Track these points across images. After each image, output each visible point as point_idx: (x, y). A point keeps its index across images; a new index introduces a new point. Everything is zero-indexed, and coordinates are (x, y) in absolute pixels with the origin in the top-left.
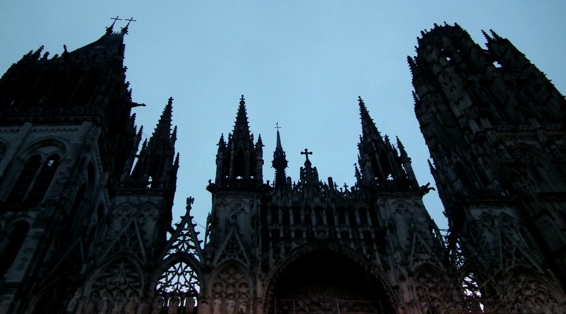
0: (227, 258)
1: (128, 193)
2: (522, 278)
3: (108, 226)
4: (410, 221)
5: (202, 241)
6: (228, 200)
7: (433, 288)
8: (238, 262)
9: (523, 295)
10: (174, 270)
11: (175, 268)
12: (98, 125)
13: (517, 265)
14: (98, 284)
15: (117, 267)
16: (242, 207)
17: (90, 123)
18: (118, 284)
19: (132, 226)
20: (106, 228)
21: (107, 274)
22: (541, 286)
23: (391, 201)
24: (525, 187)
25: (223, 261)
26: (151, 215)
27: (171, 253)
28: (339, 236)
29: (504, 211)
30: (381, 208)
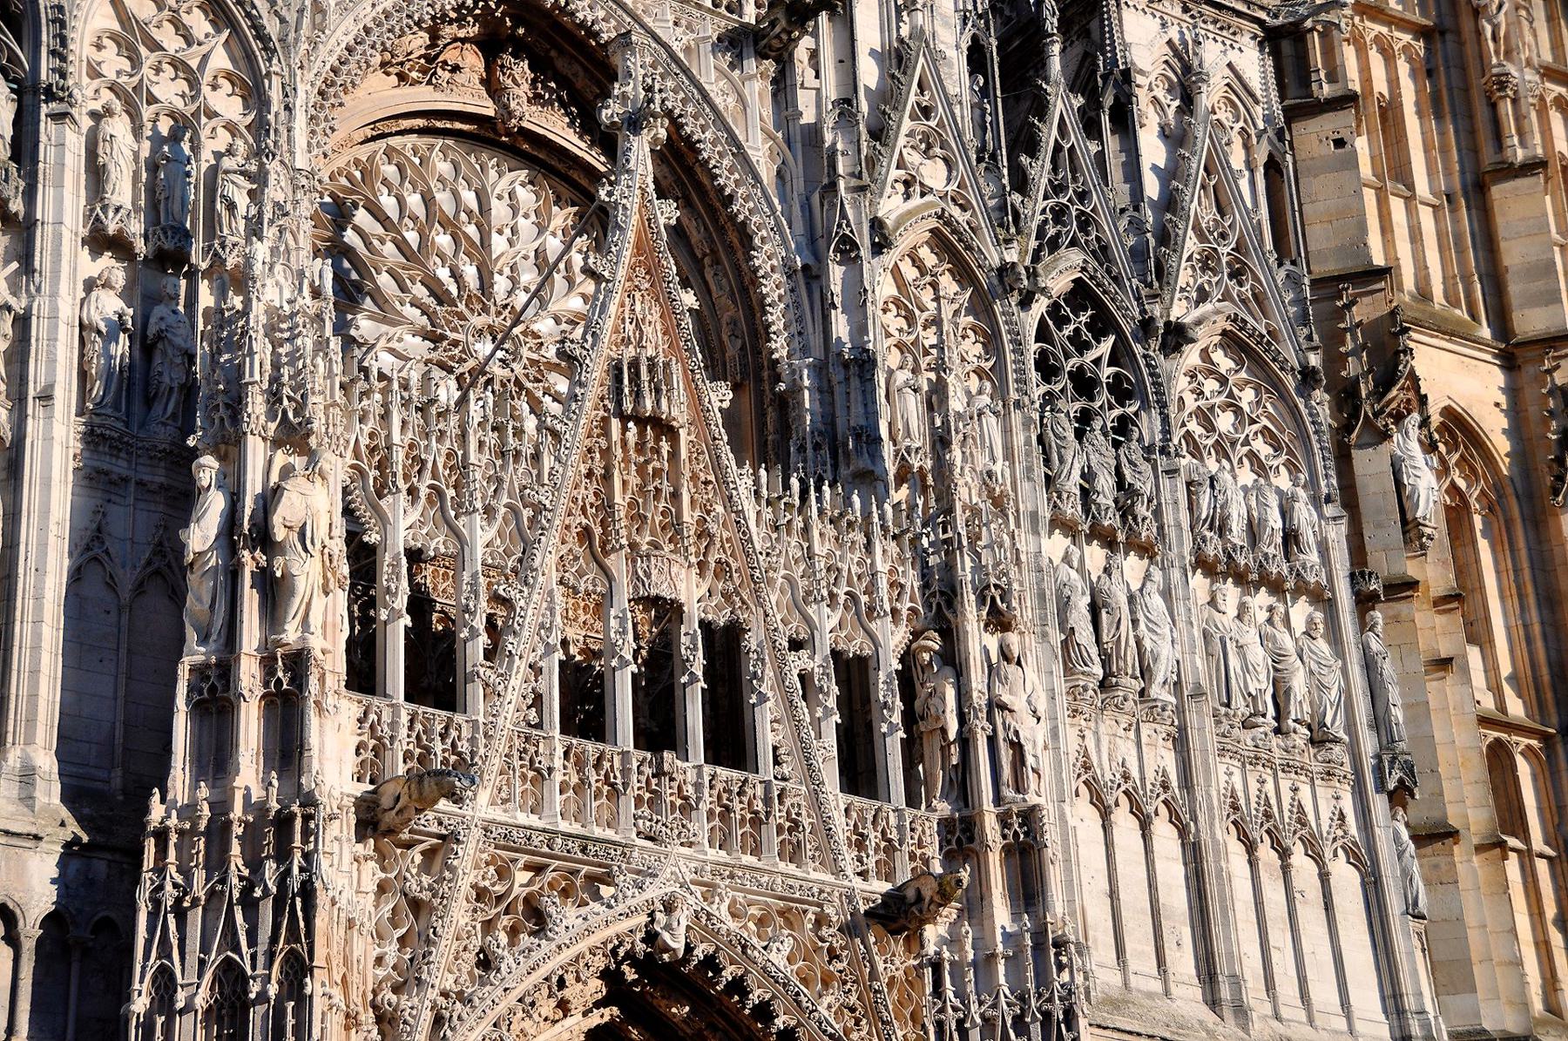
2: (1224, 362)
9: (1210, 427)
29: (1233, 56)
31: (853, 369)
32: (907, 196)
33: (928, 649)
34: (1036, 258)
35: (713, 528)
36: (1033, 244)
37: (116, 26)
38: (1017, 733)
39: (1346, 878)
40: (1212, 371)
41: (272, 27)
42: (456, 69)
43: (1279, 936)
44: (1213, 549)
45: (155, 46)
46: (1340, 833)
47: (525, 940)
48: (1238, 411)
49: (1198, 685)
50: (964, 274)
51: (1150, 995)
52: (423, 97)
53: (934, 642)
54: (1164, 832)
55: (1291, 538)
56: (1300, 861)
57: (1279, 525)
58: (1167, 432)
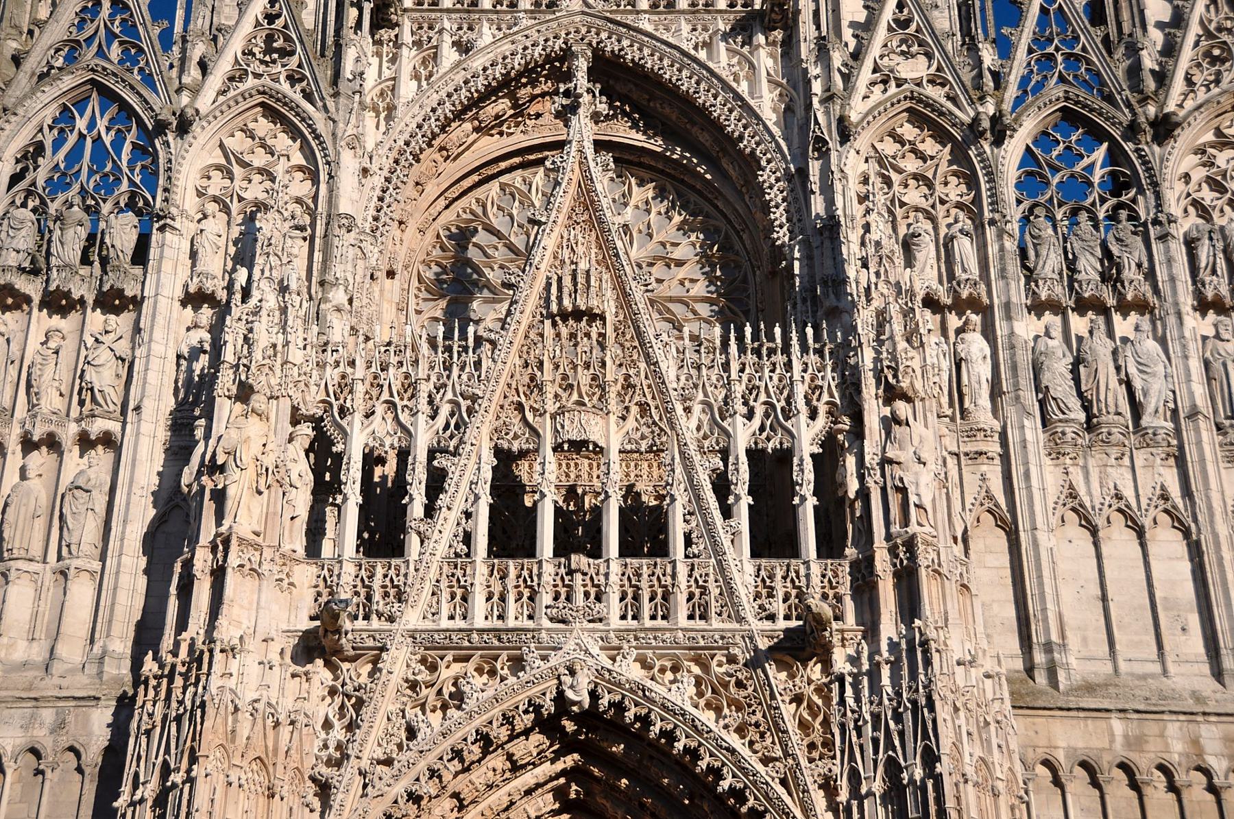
7: (916, 177)
31: (826, 234)
32: (885, 90)
33: (841, 431)
34: (1019, 101)
36: (1012, 92)
37: (223, 161)
38: (901, 480)
41: (321, 127)
42: (538, 116)
45: (244, 164)
47: (452, 712)
49: (1194, 406)
50: (941, 136)
51: (1144, 677)
52: (518, 139)
53: (846, 423)
58: (1159, 206)
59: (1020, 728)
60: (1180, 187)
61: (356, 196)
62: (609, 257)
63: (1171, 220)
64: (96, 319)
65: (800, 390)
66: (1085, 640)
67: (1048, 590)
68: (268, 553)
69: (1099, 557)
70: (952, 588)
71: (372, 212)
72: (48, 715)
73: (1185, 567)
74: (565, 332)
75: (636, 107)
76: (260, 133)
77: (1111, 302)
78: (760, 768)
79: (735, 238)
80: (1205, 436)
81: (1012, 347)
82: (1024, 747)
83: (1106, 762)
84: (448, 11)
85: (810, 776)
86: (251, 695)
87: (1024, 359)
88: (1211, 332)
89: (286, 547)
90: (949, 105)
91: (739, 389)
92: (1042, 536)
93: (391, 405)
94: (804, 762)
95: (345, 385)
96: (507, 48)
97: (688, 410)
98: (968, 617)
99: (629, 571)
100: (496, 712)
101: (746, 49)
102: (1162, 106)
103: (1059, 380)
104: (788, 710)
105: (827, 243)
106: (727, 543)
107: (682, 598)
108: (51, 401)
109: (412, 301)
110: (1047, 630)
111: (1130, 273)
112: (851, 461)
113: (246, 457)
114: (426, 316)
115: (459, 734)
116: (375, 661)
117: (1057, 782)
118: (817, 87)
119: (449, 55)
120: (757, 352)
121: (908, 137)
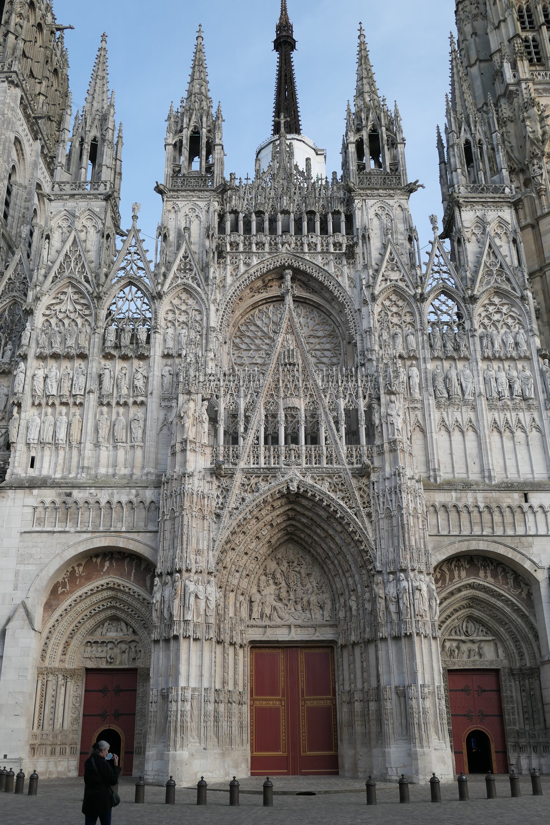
0: (179, 281)
1: (64, 197)
2: (496, 300)
3: (49, 243)
4: (386, 231)
5: (151, 261)
6: (180, 204)
7: (396, 313)
8: (192, 288)
9: (490, 319)
10: (124, 295)
11: (124, 293)
12: (17, 86)
13: (496, 285)
14: (48, 312)
15: (65, 293)
16: (197, 213)
17: (6, 84)
18: (68, 312)
19: (74, 242)
20: (47, 245)
21: (54, 301)
22: (513, 309)
23: (370, 202)
24: (542, 174)
25: (174, 285)
26: (94, 226)
27: (119, 276)
28: (306, 249)
29: (500, 214)
30: (356, 211)
35: (308, 386)
39: (534, 435)
40: (492, 304)
43: (509, 455)
44: (489, 353)
46: (533, 424)
48: (501, 312)
50: (403, 299)
52: (265, 295)
54: (470, 435)
55: (517, 344)
56: (519, 434)
57: (512, 341)
58: (472, 325)
59: (425, 495)
60: (477, 318)
61: (215, 320)
62: (299, 345)
63: (475, 330)
64: (136, 363)
65: (360, 390)
66: (445, 467)
67: (435, 452)
68: (197, 444)
69: (451, 441)
70: (407, 455)
71: (219, 323)
72: (134, 491)
73: (475, 444)
74: (286, 370)
75: (304, 283)
76: (183, 298)
77: (456, 357)
78: (349, 510)
79: (336, 329)
80: (483, 402)
81: (426, 373)
82: (426, 501)
83: (450, 505)
84: (242, 252)
85: (363, 512)
86: (196, 489)
87: (430, 376)
88: (486, 367)
89: (203, 442)
90: (407, 289)
91: (341, 389)
92: (434, 435)
93: (232, 394)
94: (362, 509)
95: (218, 387)
96: (262, 266)
97: (325, 396)
98: (411, 465)
99: (308, 449)
100: (269, 493)
101: (340, 266)
102: (473, 291)
103: (440, 383)
104: (356, 493)
105: (368, 336)
106: (338, 440)
107: (324, 458)
108: (124, 391)
109: (231, 351)
110: (434, 465)
111: (463, 348)
112: (377, 415)
113: (190, 415)
114: (235, 356)
115: (258, 500)
116: (231, 477)
117: (436, 512)
118: (364, 282)
119: (242, 268)
120: (347, 377)
121: (394, 299)
